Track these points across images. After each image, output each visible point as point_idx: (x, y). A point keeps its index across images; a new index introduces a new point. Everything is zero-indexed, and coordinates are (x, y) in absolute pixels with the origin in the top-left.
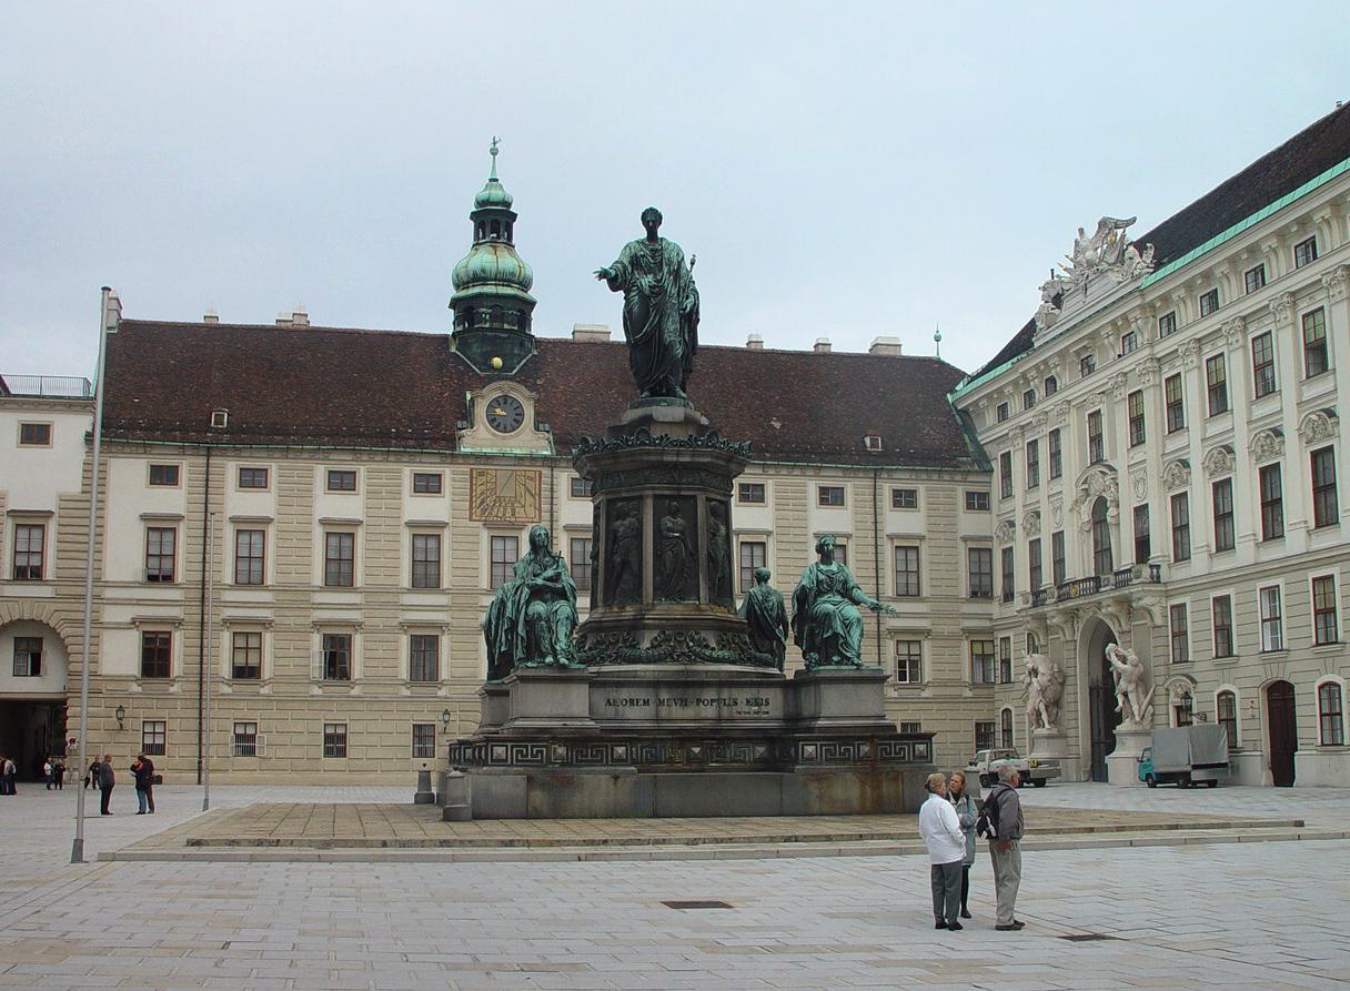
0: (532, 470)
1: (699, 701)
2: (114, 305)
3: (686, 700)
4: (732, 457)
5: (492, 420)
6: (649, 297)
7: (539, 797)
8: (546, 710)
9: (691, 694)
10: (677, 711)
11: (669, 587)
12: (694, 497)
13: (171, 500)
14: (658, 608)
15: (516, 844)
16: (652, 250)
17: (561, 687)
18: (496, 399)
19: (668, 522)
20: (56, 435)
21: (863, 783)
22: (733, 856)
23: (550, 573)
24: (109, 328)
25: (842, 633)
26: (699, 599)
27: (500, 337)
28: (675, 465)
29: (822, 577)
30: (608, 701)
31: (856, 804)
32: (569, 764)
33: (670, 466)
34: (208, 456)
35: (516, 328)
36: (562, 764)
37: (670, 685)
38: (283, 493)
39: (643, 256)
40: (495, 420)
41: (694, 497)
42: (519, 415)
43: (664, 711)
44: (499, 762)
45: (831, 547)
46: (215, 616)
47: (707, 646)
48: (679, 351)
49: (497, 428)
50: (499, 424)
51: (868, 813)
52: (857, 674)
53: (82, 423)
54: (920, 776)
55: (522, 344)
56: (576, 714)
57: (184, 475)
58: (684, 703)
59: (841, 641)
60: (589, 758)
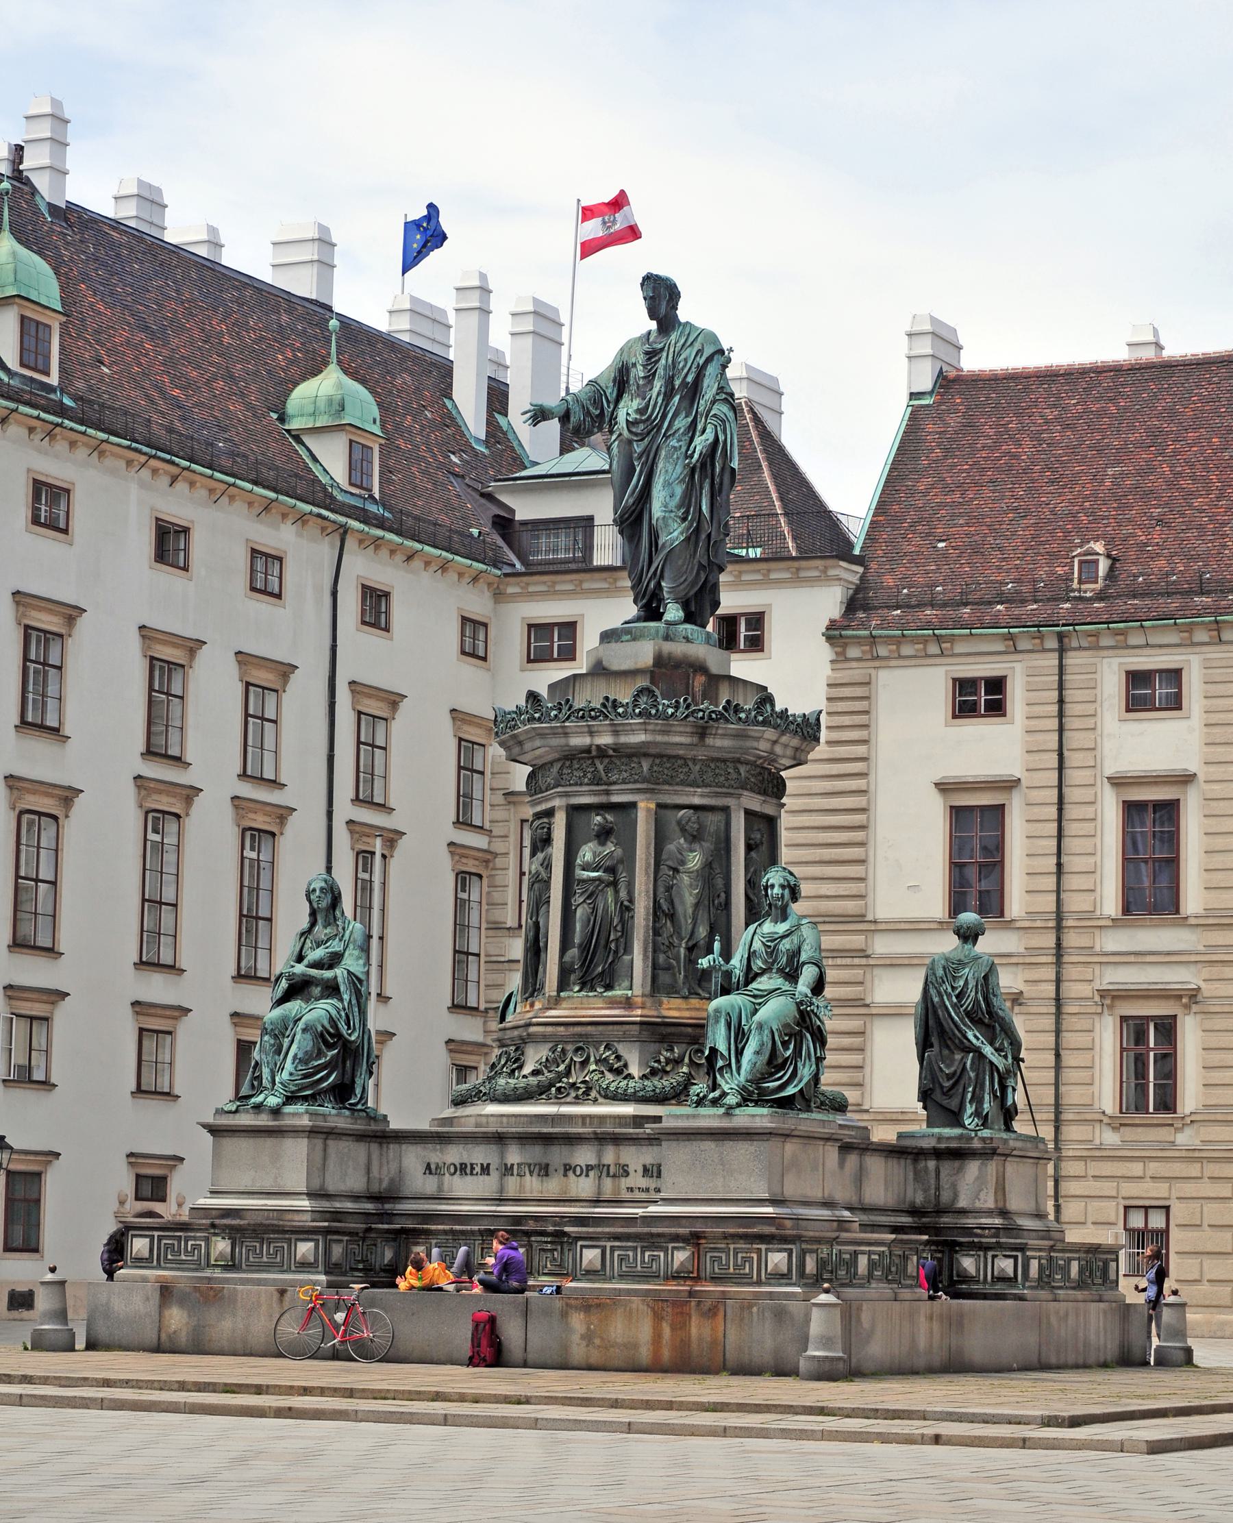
1: (568, 1168)
2: (925, 346)
3: (547, 1165)
4: (704, 728)
6: (630, 442)
7: (177, 1318)
8: (245, 1182)
9: (557, 1155)
11: (594, 965)
12: (633, 805)
13: (992, 750)
14: (564, 1005)
15: (176, 1386)
16: (647, 353)
17: (269, 1142)
20: (774, 633)
21: (658, 1318)
22: (41, 1403)
24: (913, 396)
25: (722, 1047)
28: (602, 752)
29: (757, 945)
30: (428, 1165)
31: (645, 1354)
32: (232, 1266)
33: (594, 753)
34: (1062, 651)
36: (226, 1268)
37: (524, 1139)
38: (1215, 718)
39: (634, 365)
41: (633, 805)
43: (512, 1186)
44: (140, 1262)
45: (777, 890)
46: (1072, 990)
47: (618, 1072)
48: (673, 534)
51: (665, 1370)
52: (725, 1124)
53: (827, 601)
54: (755, 1309)
56: (292, 1190)
57: (1017, 696)
58: (544, 1171)
59: (720, 1063)
60: (265, 1259)
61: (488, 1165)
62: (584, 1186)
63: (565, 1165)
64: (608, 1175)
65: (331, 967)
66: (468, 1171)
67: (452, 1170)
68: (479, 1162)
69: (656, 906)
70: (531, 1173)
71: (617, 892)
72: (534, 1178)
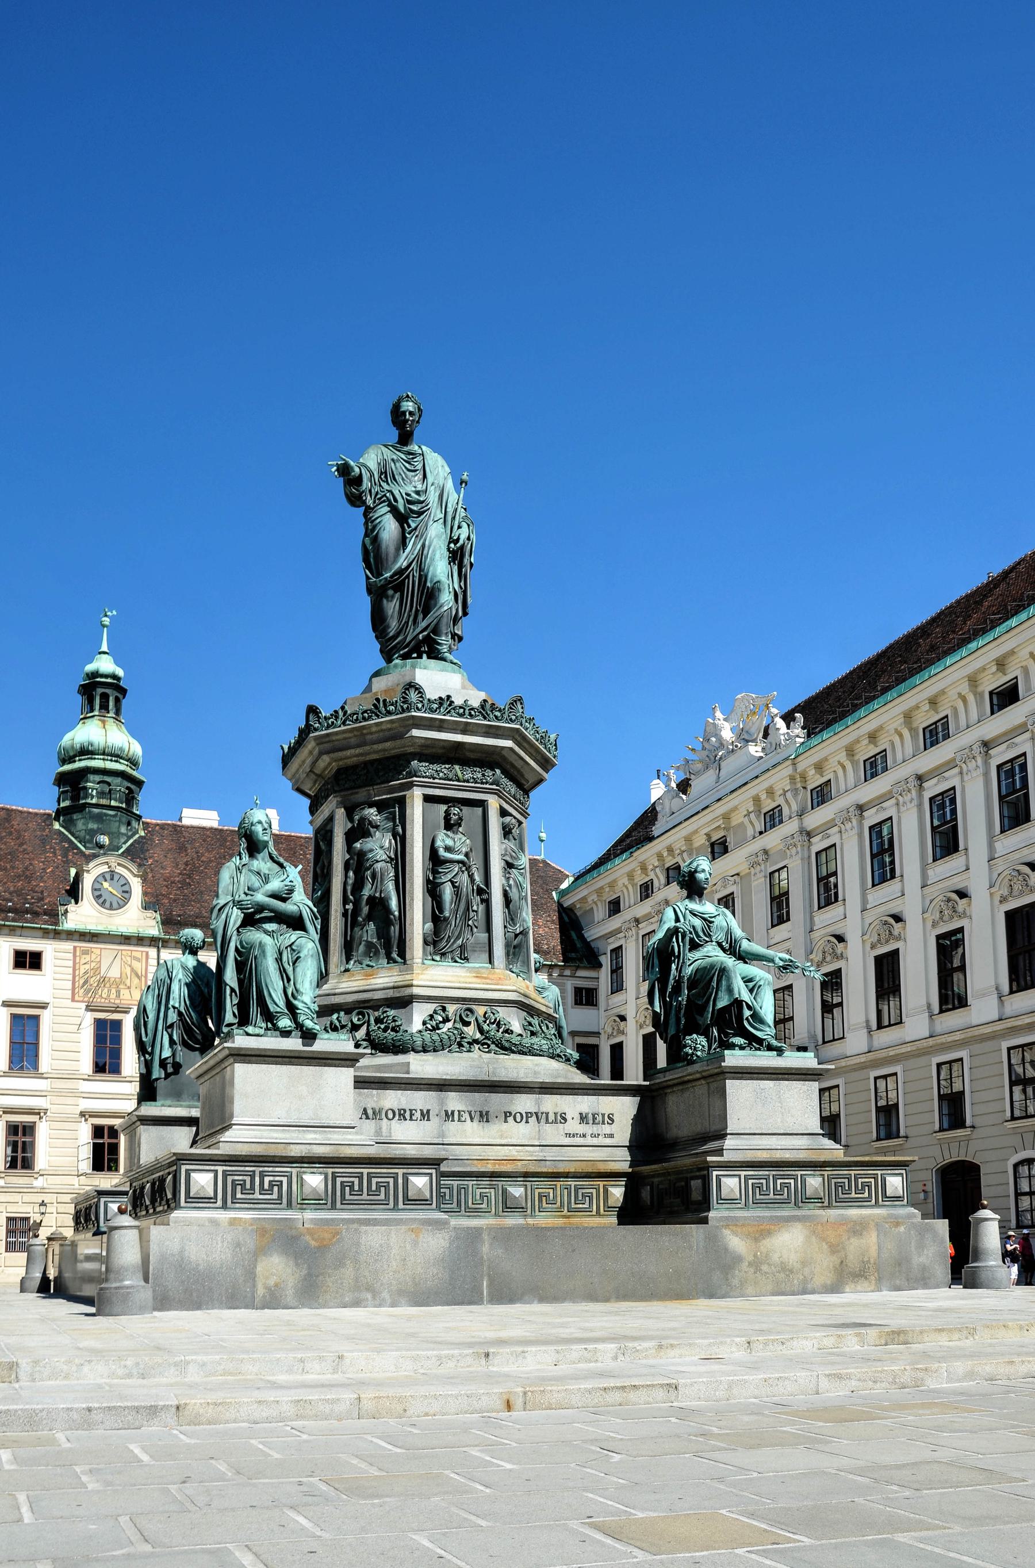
0: (138, 951)
1: (507, 1114)
3: (487, 1113)
5: (97, 895)
7: (276, 1269)
9: (497, 1101)
10: (471, 1131)
18: (103, 875)
19: (443, 839)
23: (275, 885)
26: (491, 961)
27: (106, 815)
30: (365, 1110)
35: (124, 806)
40: (100, 896)
42: (127, 892)
49: (103, 904)
50: (105, 901)
55: (129, 824)
58: (484, 1117)
61: (428, 1111)
62: (520, 1132)
63: (505, 1113)
64: (547, 1122)
65: (284, 900)
66: (408, 1117)
67: (390, 1115)
68: (419, 1107)
69: (506, 894)
70: (472, 1119)
71: (471, 876)
72: (476, 1123)
